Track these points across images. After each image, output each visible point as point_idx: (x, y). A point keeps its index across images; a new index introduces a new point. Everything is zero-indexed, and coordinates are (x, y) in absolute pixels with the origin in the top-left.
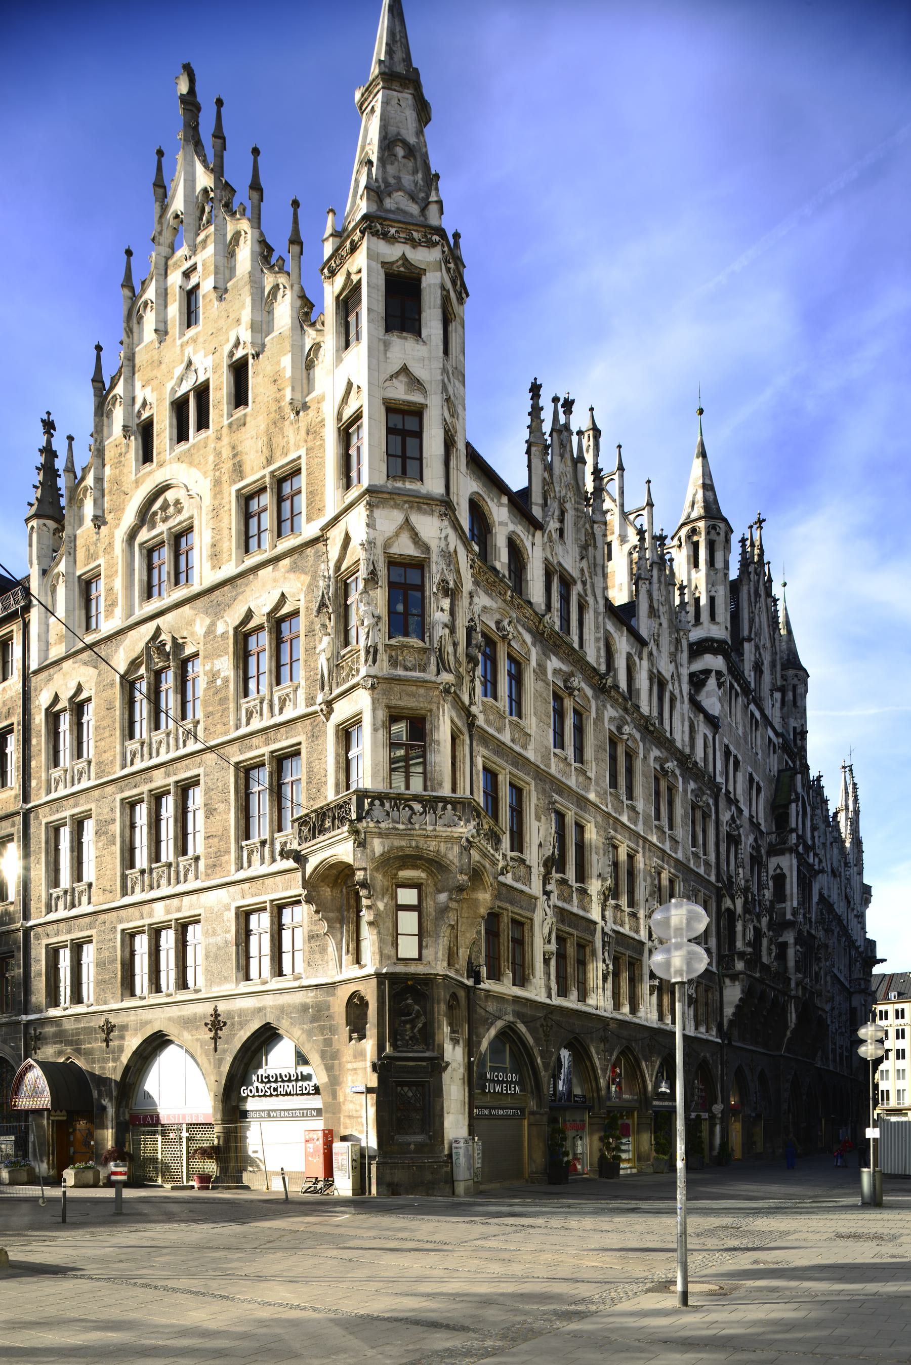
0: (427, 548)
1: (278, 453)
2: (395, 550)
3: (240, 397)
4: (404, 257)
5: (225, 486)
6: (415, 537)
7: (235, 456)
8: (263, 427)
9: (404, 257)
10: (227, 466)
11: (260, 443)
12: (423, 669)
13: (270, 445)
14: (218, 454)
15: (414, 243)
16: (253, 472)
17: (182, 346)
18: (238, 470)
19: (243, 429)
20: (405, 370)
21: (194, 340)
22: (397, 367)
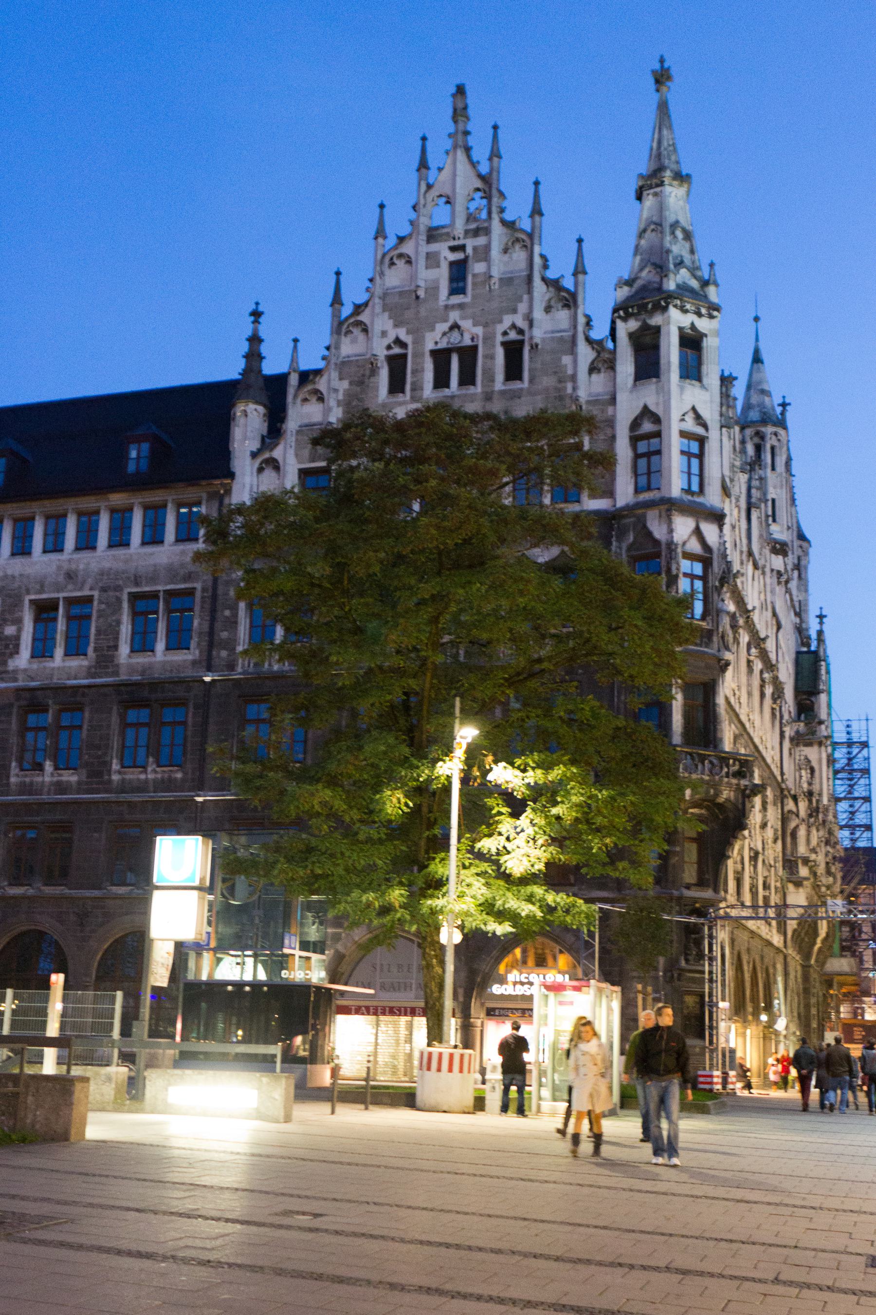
3: (513, 371)
4: (692, 324)
9: (692, 324)
15: (699, 314)
19: (517, 401)
21: (461, 306)
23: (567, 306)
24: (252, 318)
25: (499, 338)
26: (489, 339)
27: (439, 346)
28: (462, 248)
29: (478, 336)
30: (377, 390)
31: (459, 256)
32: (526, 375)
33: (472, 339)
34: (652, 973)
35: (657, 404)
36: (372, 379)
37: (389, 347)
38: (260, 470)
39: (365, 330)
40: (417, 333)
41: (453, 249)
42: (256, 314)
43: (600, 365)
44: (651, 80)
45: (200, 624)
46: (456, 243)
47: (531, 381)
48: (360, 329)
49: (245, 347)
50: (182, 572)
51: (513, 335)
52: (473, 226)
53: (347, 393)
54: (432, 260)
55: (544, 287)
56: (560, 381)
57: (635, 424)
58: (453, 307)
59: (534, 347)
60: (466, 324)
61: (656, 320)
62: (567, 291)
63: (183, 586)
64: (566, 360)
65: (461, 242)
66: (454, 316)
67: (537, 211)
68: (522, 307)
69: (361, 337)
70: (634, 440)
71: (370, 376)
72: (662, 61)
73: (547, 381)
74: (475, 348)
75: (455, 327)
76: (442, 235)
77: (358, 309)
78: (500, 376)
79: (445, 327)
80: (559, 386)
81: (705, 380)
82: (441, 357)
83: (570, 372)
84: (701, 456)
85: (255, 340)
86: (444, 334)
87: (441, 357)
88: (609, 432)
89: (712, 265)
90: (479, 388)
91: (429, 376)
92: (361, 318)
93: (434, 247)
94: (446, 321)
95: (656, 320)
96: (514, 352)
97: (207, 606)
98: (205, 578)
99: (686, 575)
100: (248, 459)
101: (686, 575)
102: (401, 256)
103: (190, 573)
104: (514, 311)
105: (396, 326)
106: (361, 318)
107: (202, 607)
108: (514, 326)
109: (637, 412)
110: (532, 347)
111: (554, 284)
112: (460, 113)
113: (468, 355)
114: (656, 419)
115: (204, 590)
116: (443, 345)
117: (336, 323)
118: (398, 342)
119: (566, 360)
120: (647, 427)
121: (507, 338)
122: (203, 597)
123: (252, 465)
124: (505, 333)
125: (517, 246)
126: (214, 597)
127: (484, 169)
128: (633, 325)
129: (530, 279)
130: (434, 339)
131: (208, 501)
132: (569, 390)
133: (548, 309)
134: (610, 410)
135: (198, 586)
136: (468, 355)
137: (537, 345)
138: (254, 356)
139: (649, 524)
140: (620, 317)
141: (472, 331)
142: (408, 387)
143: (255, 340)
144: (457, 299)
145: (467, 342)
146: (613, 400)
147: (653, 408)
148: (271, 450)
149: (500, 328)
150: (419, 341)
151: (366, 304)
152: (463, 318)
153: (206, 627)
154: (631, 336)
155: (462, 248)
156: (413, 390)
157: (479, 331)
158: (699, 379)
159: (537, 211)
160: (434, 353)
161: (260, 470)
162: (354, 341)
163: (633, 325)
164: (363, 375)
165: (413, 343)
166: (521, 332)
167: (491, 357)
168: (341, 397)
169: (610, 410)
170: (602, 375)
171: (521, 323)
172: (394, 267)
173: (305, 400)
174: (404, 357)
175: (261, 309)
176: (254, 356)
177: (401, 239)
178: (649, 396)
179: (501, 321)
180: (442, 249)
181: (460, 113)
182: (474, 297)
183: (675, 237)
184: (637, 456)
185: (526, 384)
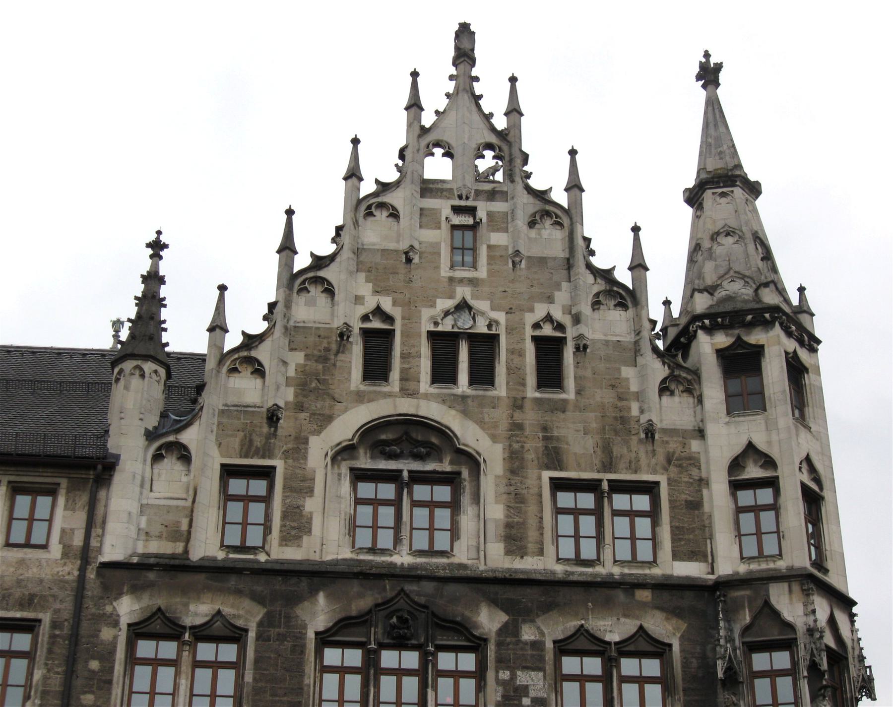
1: (622, 465)
4: (795, 352)
5: (532, 473)
9: (795, 352)
10: (533, 446)
13: (607, 448)
15: (801, 343)
16: (579, 468)
18: (553, 456)
21: (473, 282)
23: (622, 305)
24: (150, 251)
25: (529, 332)
27: (440, 328)
28: (472, 211)
29: (497, 323)
30: (350, 373)
32: (570, 383)
33: (489, 326)
35: (769, 443)
36: (341, 357)
37: (365, 318)
38: (157, 457)
39: (330, 291)
40: (410, 306)
41: (457, 210)
42: (157, 247)
43: (673, 387)
45: (45, 678)
46: (463, 203)
47: (578, 392)
48: (320, 288)
49: (139, 289)
50: (17, 593)
51: (547, 331)
52: (488, 187)
53: (302, 370)
54: (427, 218)
55: (590, 278)
56: (620, 399)
57: (736, 465)
58: (461, 281)
59: (581, 349)
60: (481, 305)
61: (756, 337)
63: (18, 615)
64: (627, 372)
65: (469, 203)
66: (463, 292)
67: (574, 186)
68: (562, 296)
69: (322, 300)
70: (736, 486)
71: (338, 352)
73: (602, 396)
74: (492, 340)
76: (442, 190)
78: (531, 379)
79: (449, 304)
80: (620, 404)
82: (443, 345)
85: (153, 279)
86: (447, 313)
87: (443, 345)
88: (695, 472)
89: (801, 290)
91: (425, 365)
92: (322, 273)
93: (430, 203)
94: (451, 297)
95: (756, 337)
96: (549, 351)
97: (61, 650)
98: (58, 606)
100: (141, 441)
102: (382, 206)
103: (32, 597)
104: (550, 300)
105: (376, 292)
106: (322, 273)
107: (50, 651)
108: (549, 318)
109: (738, 449)
110: (577, 348)
112: (464, 55)
113: (484, 346)
114: (769, 462)
115: (55, 625)
116: (447, 326)
117: (286, 276)
118: (378, 311)
119: (627, 372)
120: (754, 471)
121: (538, 333)
122: (53, 637)
123: (147, 448)
124: (537, 326)
125: (548, 222)
126: (75, 638)
128: (723, 340)
129: (569, 264)
130: (433, 315)
131: (68, 492)
132: (635, 412)
133: (596, 304)
134: (695, 445)
135: (46, 618)
136: (484, 346)
137: (585, 347)
138: (150, 301)
139: (773, 601)
140: (703, 328)
141: (488, 315)
142: (395, 375)
143: (153, 279)
145: (481, 328)
146: (701, 433)
147: (762, 446)
148: (178, 431)
149: (530, 319)
150: (410, 318)
151: (332, 258)
152: (474, 297)
153: (56, 682)
154: (721, 353)
155: (472, 211)
157: (501, 317)
160: (433, 336)
161: (157, 457)
162: (311, 303)
163: (723, 340)
164: (327, 350)
165: (403, 318)
166: (560, 327)
168: (291, 373)
170: (676, 399)
171: (558, 315)
172: (371, 219)
173: (234, 370)
174: (389, 334)
175: (163, 239)
176: (150, 301)
177: (384, 187)
178: (753, 429)
179: (532, 310)
180: (444, 207)
181: (464, 55)
182: (491, 273)
184: (740, 510)
185: (570, 393)
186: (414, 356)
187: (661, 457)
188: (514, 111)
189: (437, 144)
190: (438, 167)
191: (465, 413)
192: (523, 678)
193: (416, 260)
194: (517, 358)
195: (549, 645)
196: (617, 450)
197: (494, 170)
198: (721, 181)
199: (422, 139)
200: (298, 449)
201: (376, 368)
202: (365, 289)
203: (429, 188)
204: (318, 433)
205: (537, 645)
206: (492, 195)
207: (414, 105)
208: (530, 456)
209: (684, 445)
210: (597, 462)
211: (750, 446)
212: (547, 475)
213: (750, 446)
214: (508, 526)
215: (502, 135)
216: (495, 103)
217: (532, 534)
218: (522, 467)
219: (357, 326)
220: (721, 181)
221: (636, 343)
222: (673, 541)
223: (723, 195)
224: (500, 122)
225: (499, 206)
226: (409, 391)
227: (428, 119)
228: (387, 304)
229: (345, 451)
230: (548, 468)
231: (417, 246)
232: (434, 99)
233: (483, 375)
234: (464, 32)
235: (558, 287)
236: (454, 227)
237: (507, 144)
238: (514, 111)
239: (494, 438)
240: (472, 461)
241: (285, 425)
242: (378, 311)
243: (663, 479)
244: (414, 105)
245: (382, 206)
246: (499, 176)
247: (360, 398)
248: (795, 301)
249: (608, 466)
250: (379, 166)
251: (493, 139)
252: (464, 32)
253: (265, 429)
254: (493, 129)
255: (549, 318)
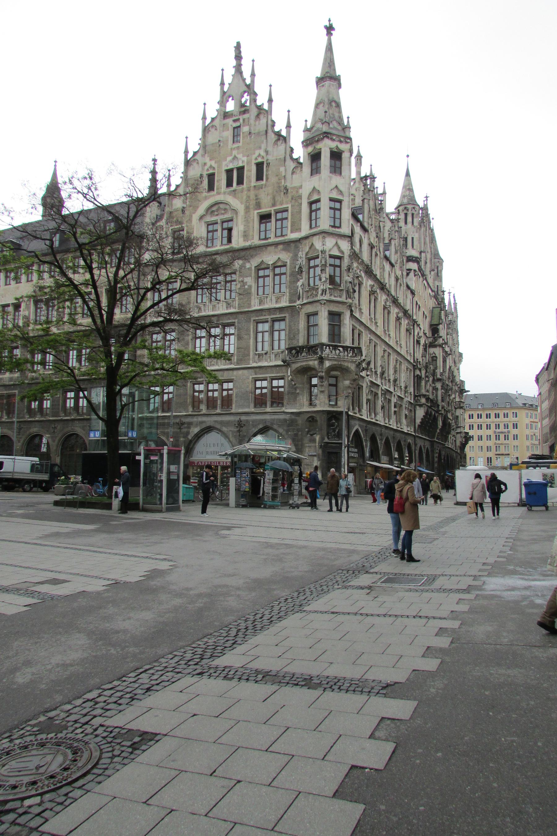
0: (342, 252)
2: (332, 253)
3: (259, 177)
4: (337, 146)
5: (252, 212)
6: (339, 248)
7: (257, 199)
8: (270, 191)
9: (337, 146)
10: (253, 203)
11: (269, 197)
12: (340, 297)
13: (274, 198)
14: (249, 197)
15: (341, 142)
17: (231, 149)
18: (258, 205)
20: (336, 187)
21: (238, 148)
22: (334, 186)
25: (254, 162)
26: (249, 163)
31: (237, 124)
34: (313, 445)
37: (208, 170)
40: (219, 163)
41: (235, 121)
44: (325, 31)
46: (235, 118)
51: (260, 160)
52: (243, 109)
57: (310, 195)
60: (240, 156)
61: (320, 146)
62: (283, 136)
64: (282, 169)
66: (235, 153)
67: (270, 101)
68: (263, 146)
72: (330, 21)
75: (235, 158)
77: (195, 153)
81: (343, 174)
82: (229, 172)
83: (283, 175)
84: (340, 210)
86: (231, 162)
87: (229, 172)
89: (348, 118)
90: (245, 186)
91: (224, 182)
96: (260, 166)
99: (330, 265)
101: (330, 265)
102: (213, 126)
104: (260, 148)
111: (278, 134)
112: (238, 57)
113: (241, 170)
114: (319, 192)
116: (231, 166)
118: (211, 167)
119: (282, 169)
120: (315, 197)
121: (257, 161)
124: (256, 159)
127: (248, 82)
129: (266, 132)
136: (241, 170)
138: (154, 180)
144: (236, 145)
147: (317, 188)
149: (254, 157)
152: (238, 154)
156: (217, 189)
157: (245, 159)
158: (341, 174)
159: (270, 101)
166: (263, 157)
167: (250, 171)
169: (300, 191)
171: (263, 153)
176: (154, 180)
180: (229, 121)
181: (238, 57)
183: (331, 105)
184: (311, 211)
186: (221, 180)
187: (290, 198)
188: (253, 75)
189: (230, 97)
190: (231, 106)
191: (235, 196)
192: (246, 280)
193: (222, 144)
194: (251, 173)
195: (253, 268)
196: (278, 199)
197: (246, 102)
198: (329, 78)
199: (224, 97)
200: (190, 220)
201: (211, 187)
202: (207, 159)
203: (226, 115)
204: (194, 213)
205: (250, 269)
206: (245, 112)
207: (222, 84)
208: (251, 207)
209: (297, 192)
210: (270, 204)
211: (314, 188)
212: (256, 212)
213: (314, 188)
214: (245, 232)
215: (248, 86)
216: (247, 74)
217: (251, 233)
218: (249, 211)
219: (205, 173)
220: (329, 78)
221: (285, 158)
222: (291, 226)
223: (323, 86)
224: (248, 82)
225: (246, 116)
226: (218, 193)
227: (226, 89)
228: (213, 163)
229: (201, 218)
230: (256, 209)
231: (221, 139)
232: (228, 80)
233: (240, 182)
234: (238, 47)
235: (263, 142)
236: (234, 128)
237: (250, 89)
238: (253, 75)
239: (242, 203)
240: (235, 211)
241: (187, 212)
242: (211, 166)
243: (289, 206)
244: (222, 84)
245: (213, 126)
246: (248, 104)
247: (206, 198)
248: (346, 124)
249: (274, 205)
250: (212, 113)
251: (245, 89)
252: (238, 47)
253: (181, 215)
254: (246, 85)
255: (259, 155)
